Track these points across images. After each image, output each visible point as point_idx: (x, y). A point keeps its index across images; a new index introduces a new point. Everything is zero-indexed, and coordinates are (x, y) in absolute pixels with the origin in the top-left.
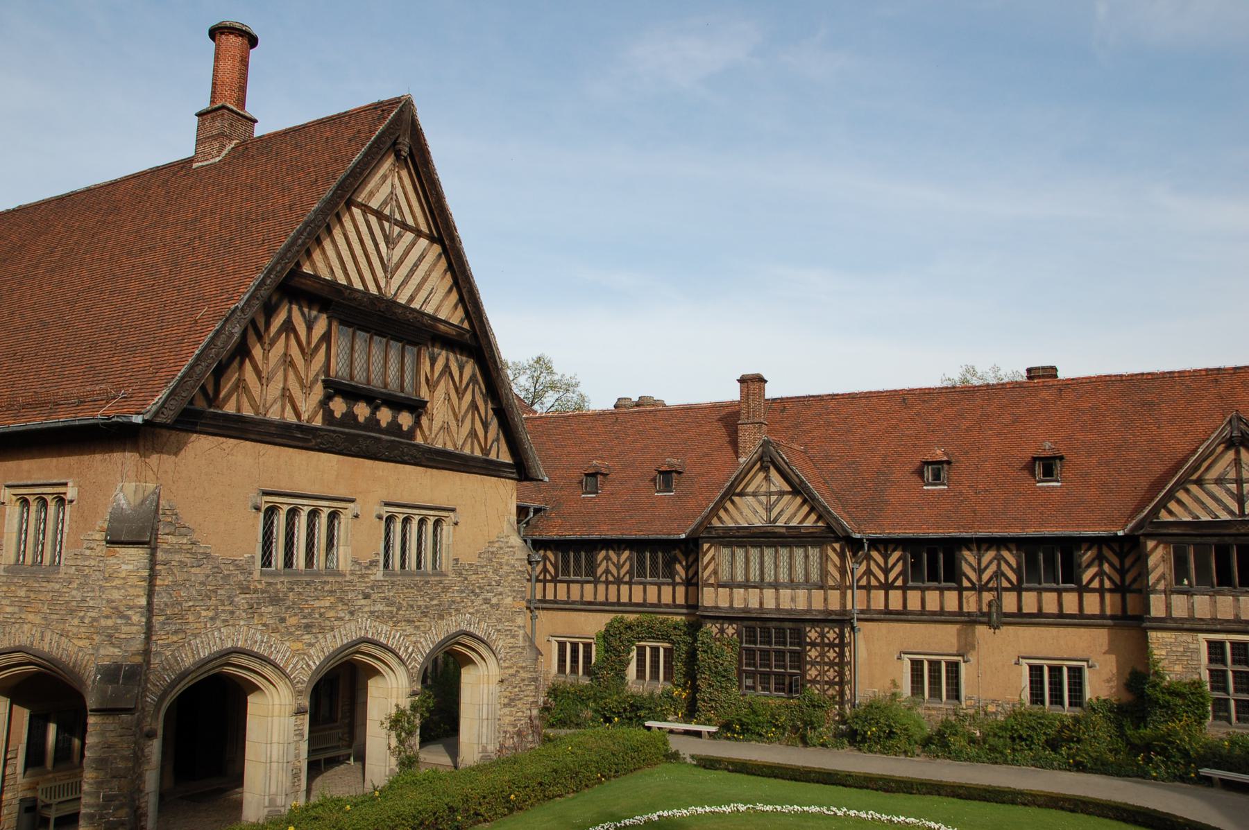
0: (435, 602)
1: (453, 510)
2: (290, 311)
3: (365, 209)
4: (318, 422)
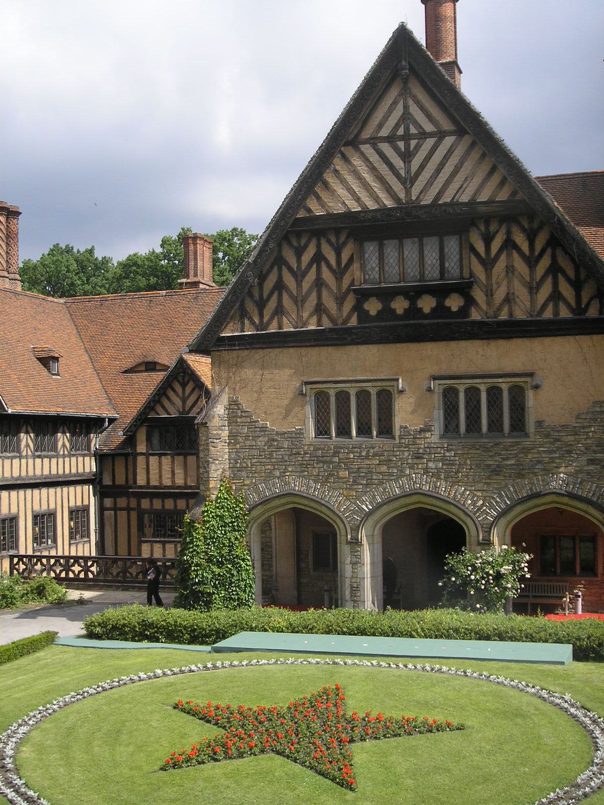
0: (513, 462)
1: (531, 375)
2: (319, 246)
3: (374, 141)
4: (353, 322)
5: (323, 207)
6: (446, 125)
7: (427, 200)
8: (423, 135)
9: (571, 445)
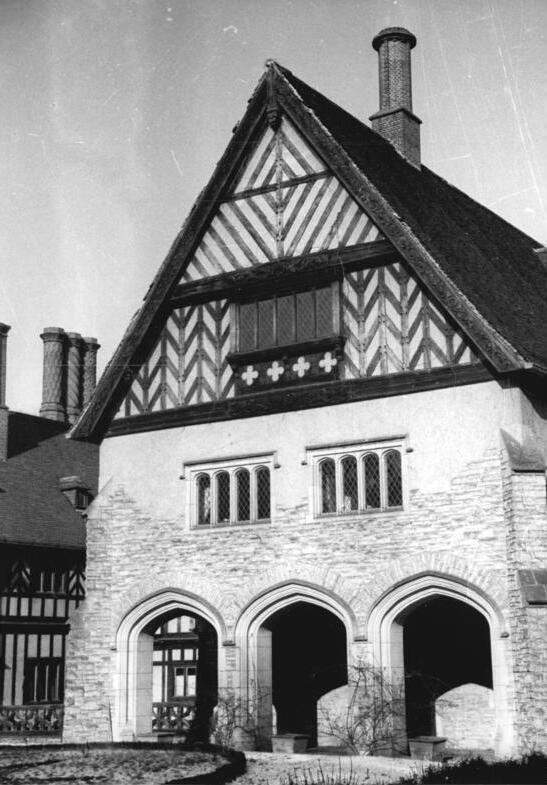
0: (388, 540)
2: (200, 316)
4: (231, 394)
5: (200, 272)
6: (317, 166)
7: (298, 251)
8: (294, 182)
9: (445, 517)
